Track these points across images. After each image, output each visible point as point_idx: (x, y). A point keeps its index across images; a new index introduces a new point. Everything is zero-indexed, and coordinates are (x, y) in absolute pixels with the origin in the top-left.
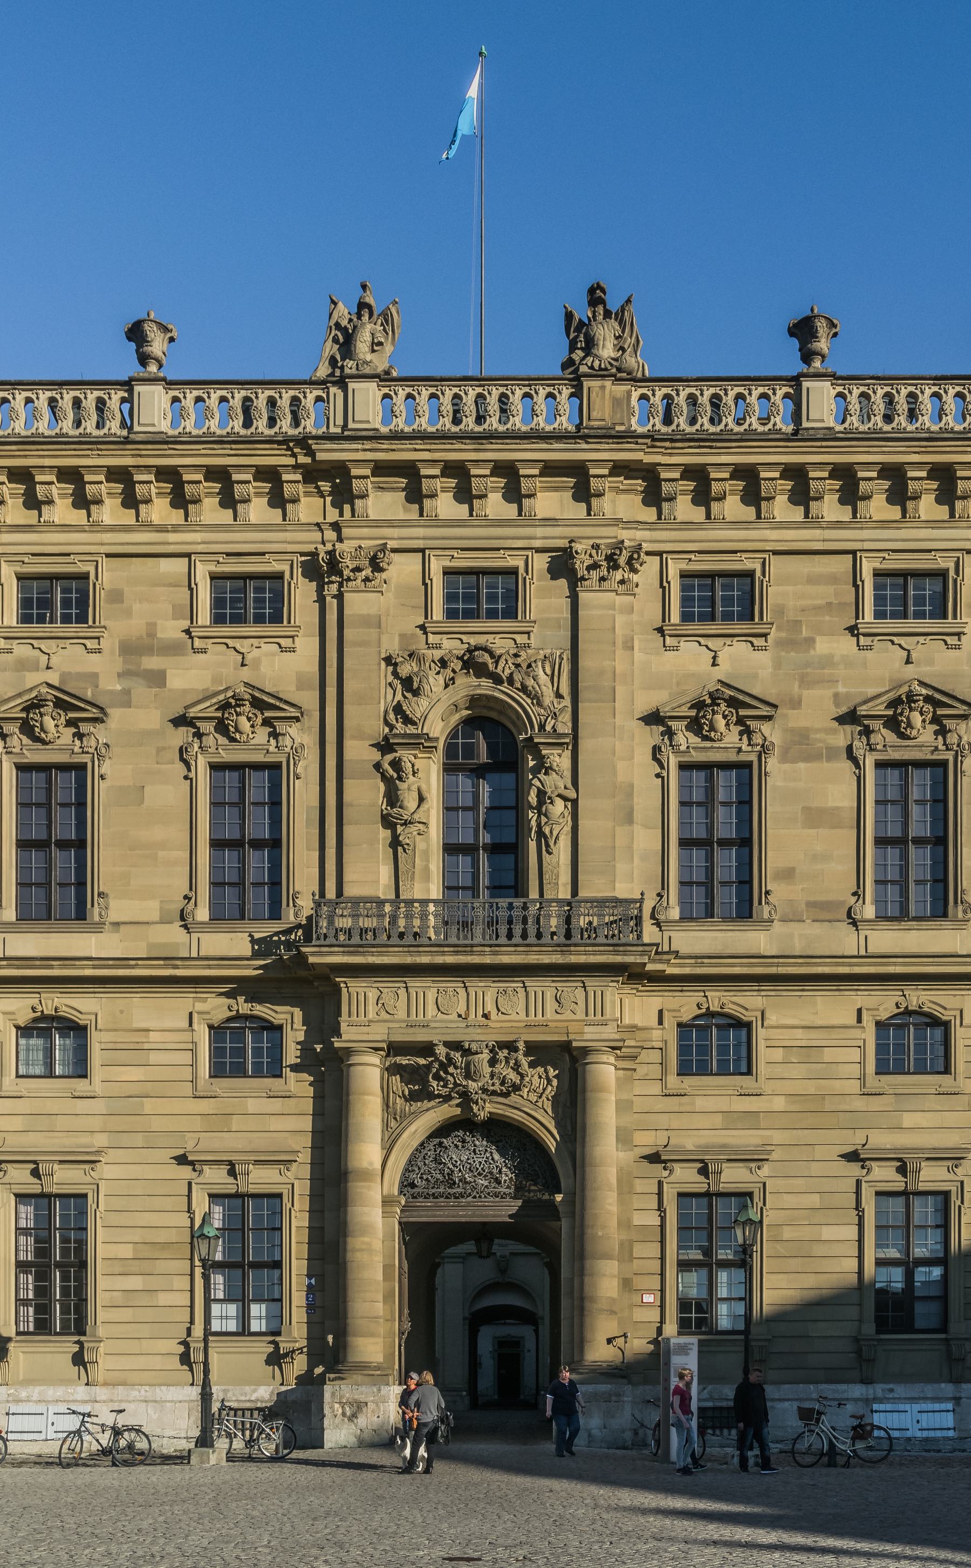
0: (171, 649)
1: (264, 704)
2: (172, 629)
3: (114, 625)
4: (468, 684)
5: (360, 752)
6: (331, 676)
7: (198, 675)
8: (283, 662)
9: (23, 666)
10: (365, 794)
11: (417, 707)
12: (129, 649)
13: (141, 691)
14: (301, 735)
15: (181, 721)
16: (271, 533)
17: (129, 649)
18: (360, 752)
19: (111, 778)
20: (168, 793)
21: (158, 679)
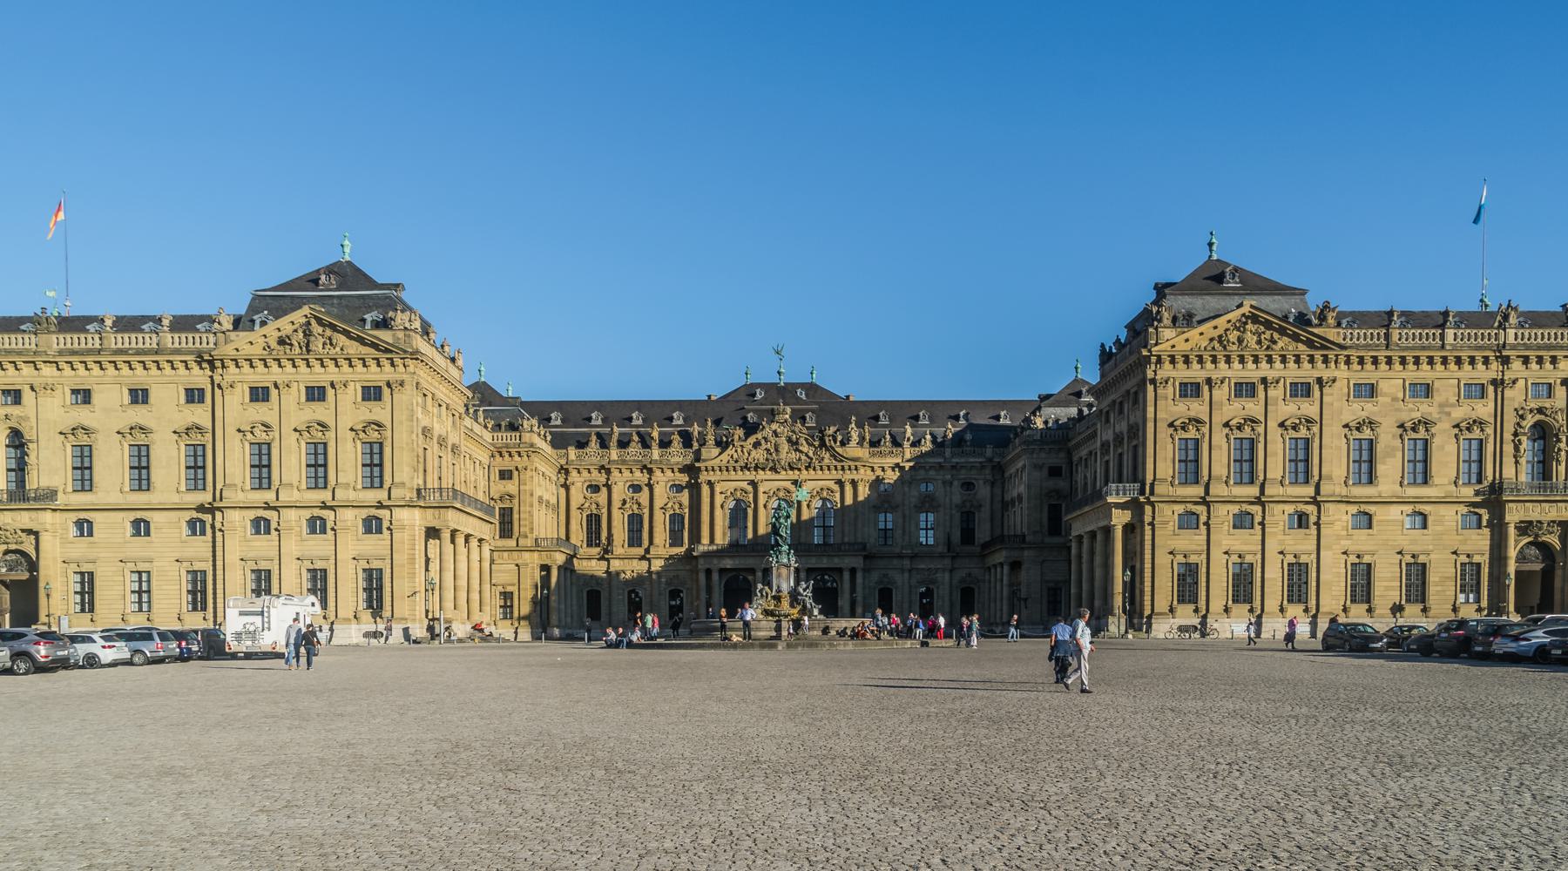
0: (1452, 405)
1: (1481, 423)
2: (1453, 400)
3: (1438, 398)
4: (1539, 417)
5: (1508, 436)
6: (1499, 414)
7: (1459, 413)
8: (1484, 409)
9: (1411, 410)
10: (1509, 448)
11: (1524, 423)
12: (1441, 405)
13: (1444, 417)
14: (1489, 430)
15: (1457, 426)
16: (1483, 374)
17: (1441, 405)
18: (1508, 436)
19: (1436, 443)
20: (1452, 447)
21: (1449, 414)
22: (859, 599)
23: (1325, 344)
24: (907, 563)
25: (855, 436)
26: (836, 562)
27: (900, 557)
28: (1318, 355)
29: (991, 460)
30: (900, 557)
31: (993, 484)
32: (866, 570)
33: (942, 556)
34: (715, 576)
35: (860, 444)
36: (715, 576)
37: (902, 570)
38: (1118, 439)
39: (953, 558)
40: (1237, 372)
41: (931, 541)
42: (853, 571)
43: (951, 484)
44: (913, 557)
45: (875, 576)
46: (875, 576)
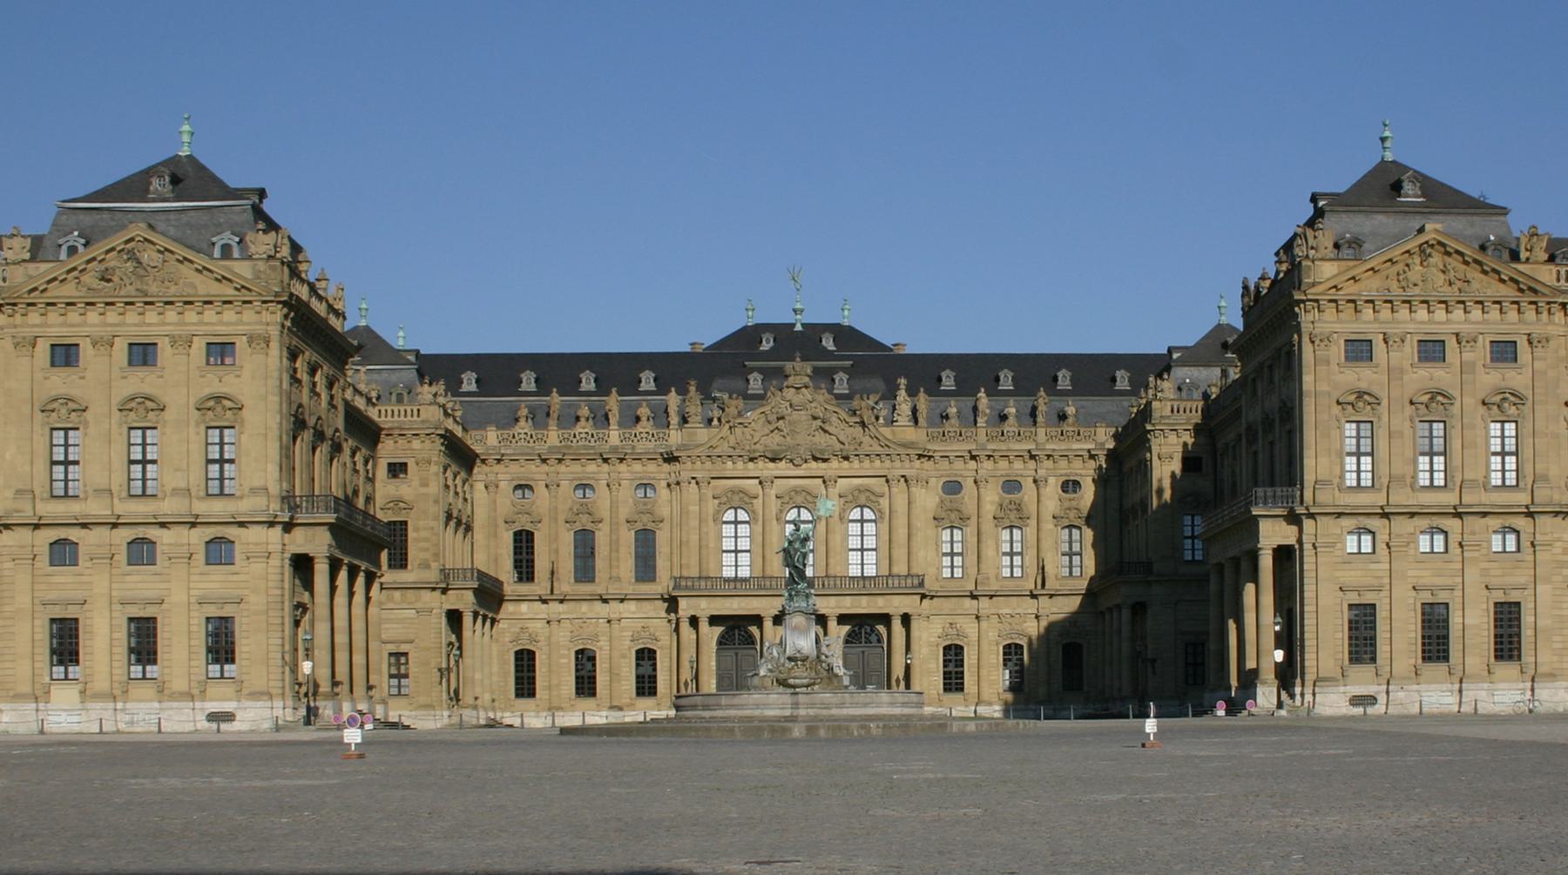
25: (904, 408)
34: (704, 626)
42: (906, 619)
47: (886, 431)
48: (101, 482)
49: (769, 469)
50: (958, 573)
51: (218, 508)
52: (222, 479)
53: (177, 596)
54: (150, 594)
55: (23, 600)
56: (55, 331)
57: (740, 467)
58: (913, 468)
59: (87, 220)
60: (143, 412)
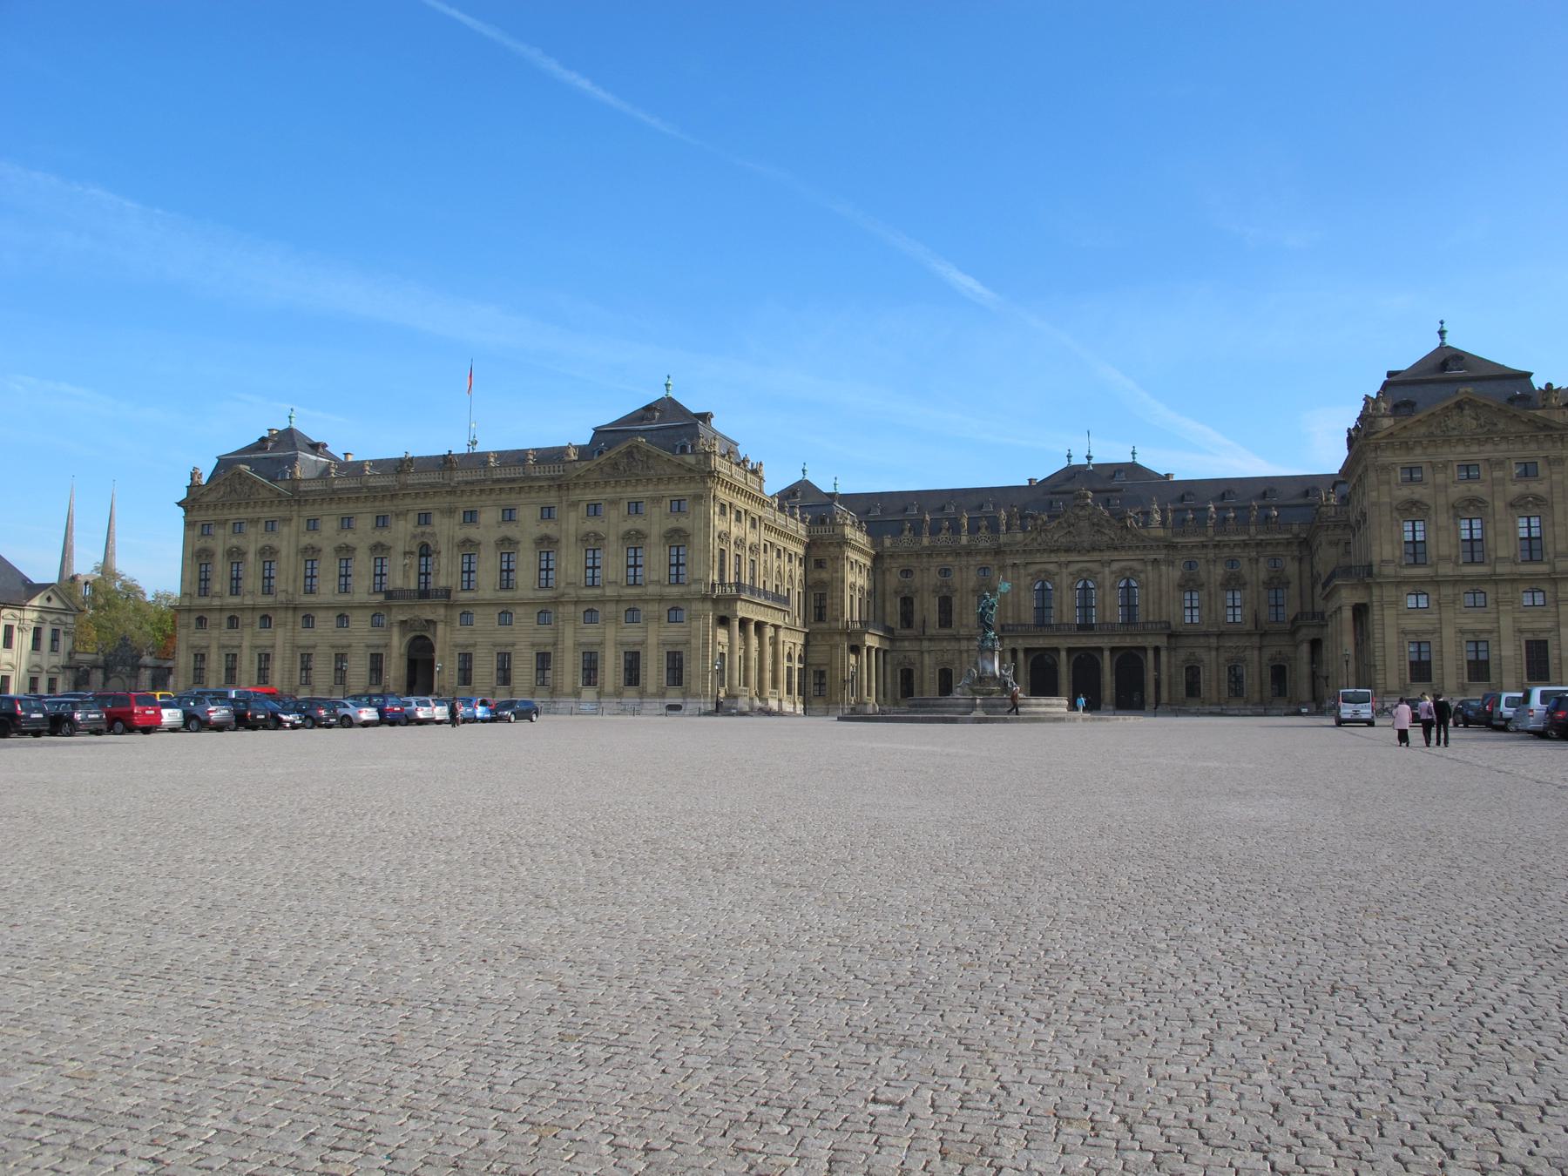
22: (1164, 677)
23: (1547, 427)
24: (1213, 641)
26: (1140, 641)
27: (1207, 635)
28: (1541, 435)
29: (1297, 536)
30: (1207, 635)
31: (1300, 560)
32: (1167, 648)
33: (1249, 634)
34: (1021, 656)
35: (1163, 523)
36: (1021, 656)
37: (1209, 648)
38: (1358, 522)
39: (1262, 635)
40: (1458, 453)
41: (1238, 619)
42: (1157, 650)
43: (1257, 561)
44: (1220, 635)
45: (1182, 655)
46: (1182, 655)
47: (1144, 532)
48: (612, 577)
49: (1063, 558)
50: (1196, 620)
51: (675, 591)
52: (678, 574)
53: (652, 640)
54: (637, 639)
55: (569, 643)
56: (589, 497)
57: (1045, 558)
58: (1161, 555)
59: (611, 436)
60: (634, 539)
